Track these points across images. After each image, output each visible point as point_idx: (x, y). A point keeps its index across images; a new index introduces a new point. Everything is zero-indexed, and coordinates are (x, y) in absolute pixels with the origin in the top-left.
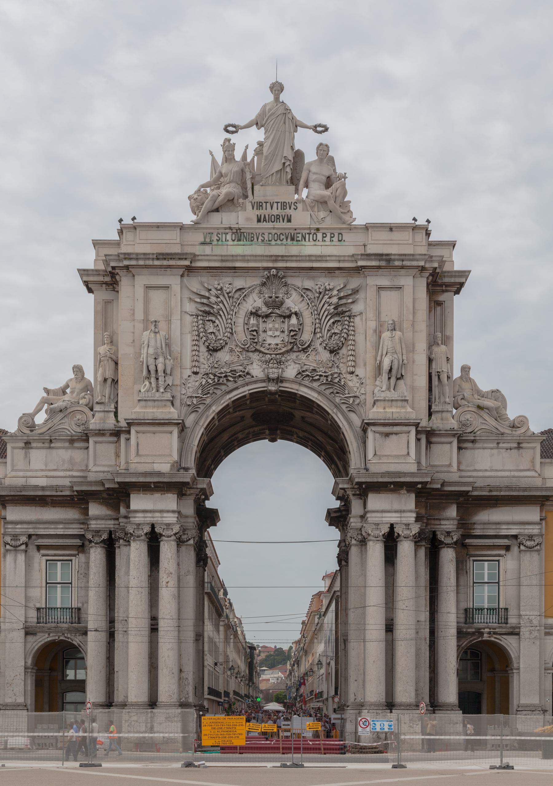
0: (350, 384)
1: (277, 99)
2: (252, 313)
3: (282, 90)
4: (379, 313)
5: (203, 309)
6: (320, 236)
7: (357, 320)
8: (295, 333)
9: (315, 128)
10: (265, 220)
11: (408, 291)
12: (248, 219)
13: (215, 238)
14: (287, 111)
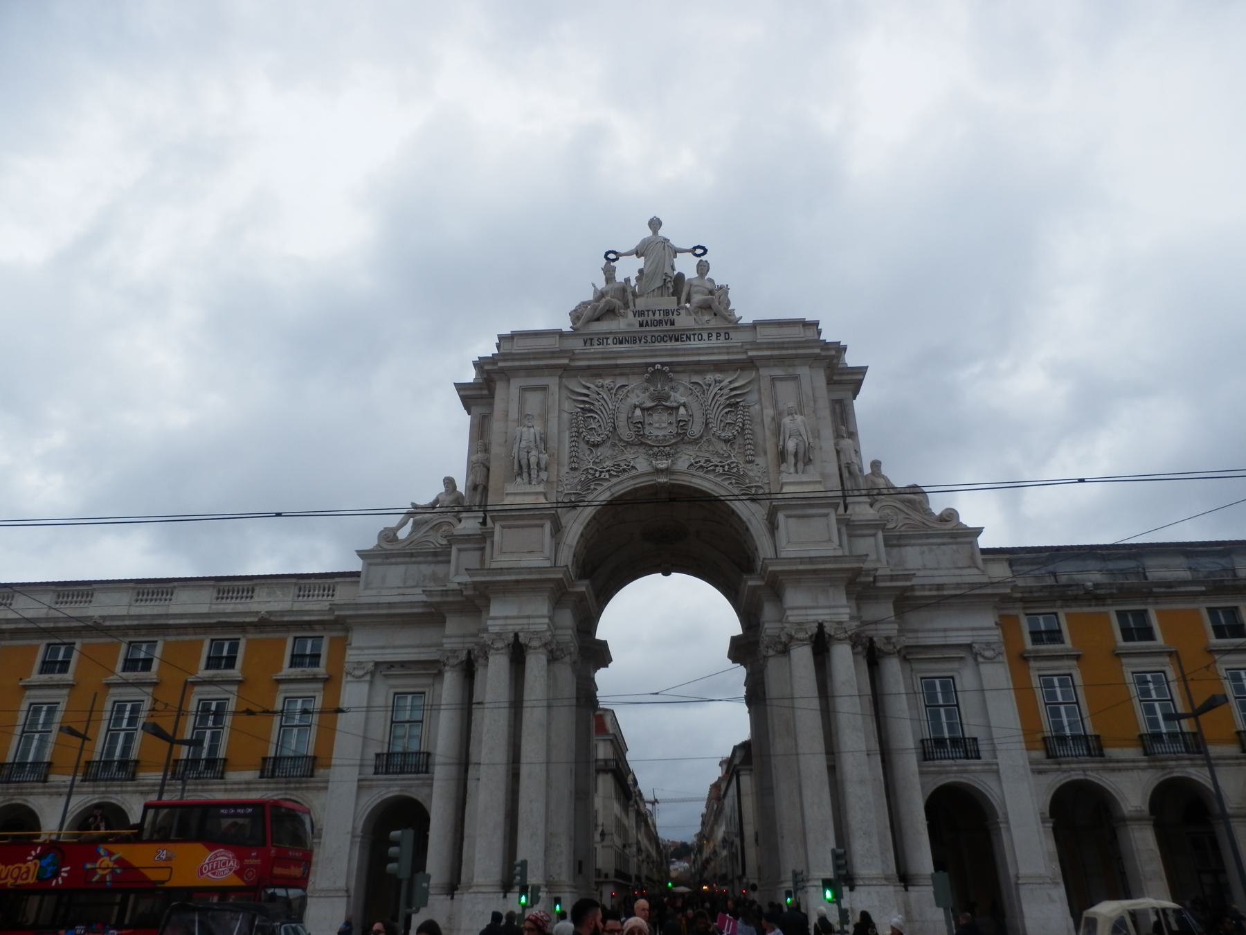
0: (751, 474)
1: (655, 232)
3: (660, 224)
4: (775, 404)
6: (705, 336)
8: (682, 425)
11: (805, 382)
12: (629, 325)
14: (666, 241)
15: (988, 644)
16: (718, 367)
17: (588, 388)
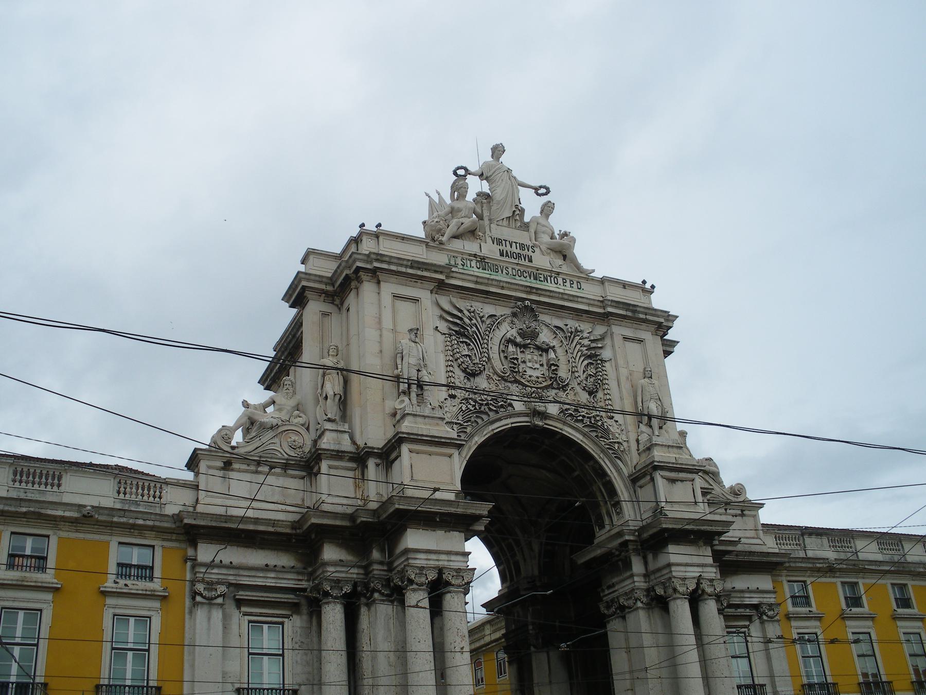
2: (510, 341)
5: (457, 329)
7: (607, 364)
8: (553, 367)
9: (536, 189)
10: (507, 255)
13: (460, 262)
15: (771, 606)
16: (578, 314)
17: (461, 311)
